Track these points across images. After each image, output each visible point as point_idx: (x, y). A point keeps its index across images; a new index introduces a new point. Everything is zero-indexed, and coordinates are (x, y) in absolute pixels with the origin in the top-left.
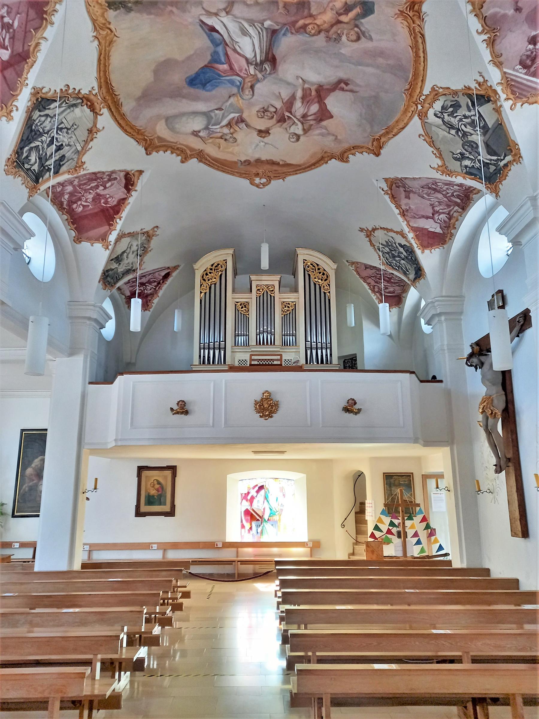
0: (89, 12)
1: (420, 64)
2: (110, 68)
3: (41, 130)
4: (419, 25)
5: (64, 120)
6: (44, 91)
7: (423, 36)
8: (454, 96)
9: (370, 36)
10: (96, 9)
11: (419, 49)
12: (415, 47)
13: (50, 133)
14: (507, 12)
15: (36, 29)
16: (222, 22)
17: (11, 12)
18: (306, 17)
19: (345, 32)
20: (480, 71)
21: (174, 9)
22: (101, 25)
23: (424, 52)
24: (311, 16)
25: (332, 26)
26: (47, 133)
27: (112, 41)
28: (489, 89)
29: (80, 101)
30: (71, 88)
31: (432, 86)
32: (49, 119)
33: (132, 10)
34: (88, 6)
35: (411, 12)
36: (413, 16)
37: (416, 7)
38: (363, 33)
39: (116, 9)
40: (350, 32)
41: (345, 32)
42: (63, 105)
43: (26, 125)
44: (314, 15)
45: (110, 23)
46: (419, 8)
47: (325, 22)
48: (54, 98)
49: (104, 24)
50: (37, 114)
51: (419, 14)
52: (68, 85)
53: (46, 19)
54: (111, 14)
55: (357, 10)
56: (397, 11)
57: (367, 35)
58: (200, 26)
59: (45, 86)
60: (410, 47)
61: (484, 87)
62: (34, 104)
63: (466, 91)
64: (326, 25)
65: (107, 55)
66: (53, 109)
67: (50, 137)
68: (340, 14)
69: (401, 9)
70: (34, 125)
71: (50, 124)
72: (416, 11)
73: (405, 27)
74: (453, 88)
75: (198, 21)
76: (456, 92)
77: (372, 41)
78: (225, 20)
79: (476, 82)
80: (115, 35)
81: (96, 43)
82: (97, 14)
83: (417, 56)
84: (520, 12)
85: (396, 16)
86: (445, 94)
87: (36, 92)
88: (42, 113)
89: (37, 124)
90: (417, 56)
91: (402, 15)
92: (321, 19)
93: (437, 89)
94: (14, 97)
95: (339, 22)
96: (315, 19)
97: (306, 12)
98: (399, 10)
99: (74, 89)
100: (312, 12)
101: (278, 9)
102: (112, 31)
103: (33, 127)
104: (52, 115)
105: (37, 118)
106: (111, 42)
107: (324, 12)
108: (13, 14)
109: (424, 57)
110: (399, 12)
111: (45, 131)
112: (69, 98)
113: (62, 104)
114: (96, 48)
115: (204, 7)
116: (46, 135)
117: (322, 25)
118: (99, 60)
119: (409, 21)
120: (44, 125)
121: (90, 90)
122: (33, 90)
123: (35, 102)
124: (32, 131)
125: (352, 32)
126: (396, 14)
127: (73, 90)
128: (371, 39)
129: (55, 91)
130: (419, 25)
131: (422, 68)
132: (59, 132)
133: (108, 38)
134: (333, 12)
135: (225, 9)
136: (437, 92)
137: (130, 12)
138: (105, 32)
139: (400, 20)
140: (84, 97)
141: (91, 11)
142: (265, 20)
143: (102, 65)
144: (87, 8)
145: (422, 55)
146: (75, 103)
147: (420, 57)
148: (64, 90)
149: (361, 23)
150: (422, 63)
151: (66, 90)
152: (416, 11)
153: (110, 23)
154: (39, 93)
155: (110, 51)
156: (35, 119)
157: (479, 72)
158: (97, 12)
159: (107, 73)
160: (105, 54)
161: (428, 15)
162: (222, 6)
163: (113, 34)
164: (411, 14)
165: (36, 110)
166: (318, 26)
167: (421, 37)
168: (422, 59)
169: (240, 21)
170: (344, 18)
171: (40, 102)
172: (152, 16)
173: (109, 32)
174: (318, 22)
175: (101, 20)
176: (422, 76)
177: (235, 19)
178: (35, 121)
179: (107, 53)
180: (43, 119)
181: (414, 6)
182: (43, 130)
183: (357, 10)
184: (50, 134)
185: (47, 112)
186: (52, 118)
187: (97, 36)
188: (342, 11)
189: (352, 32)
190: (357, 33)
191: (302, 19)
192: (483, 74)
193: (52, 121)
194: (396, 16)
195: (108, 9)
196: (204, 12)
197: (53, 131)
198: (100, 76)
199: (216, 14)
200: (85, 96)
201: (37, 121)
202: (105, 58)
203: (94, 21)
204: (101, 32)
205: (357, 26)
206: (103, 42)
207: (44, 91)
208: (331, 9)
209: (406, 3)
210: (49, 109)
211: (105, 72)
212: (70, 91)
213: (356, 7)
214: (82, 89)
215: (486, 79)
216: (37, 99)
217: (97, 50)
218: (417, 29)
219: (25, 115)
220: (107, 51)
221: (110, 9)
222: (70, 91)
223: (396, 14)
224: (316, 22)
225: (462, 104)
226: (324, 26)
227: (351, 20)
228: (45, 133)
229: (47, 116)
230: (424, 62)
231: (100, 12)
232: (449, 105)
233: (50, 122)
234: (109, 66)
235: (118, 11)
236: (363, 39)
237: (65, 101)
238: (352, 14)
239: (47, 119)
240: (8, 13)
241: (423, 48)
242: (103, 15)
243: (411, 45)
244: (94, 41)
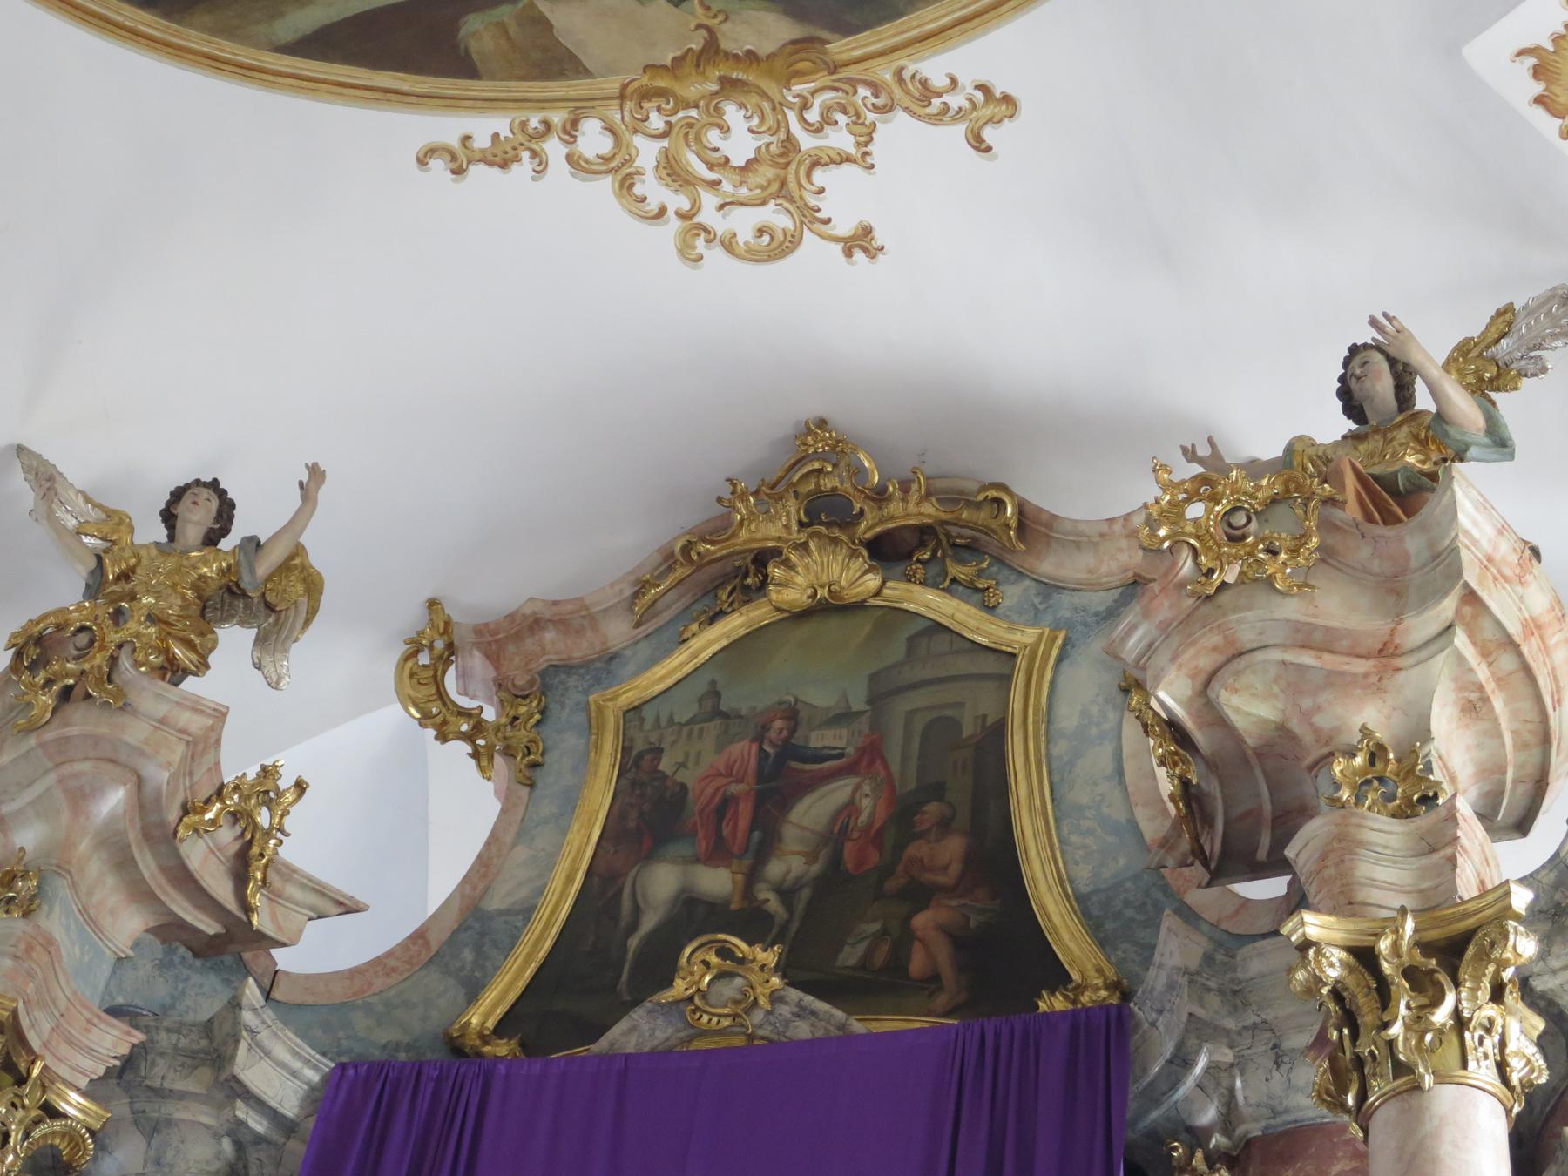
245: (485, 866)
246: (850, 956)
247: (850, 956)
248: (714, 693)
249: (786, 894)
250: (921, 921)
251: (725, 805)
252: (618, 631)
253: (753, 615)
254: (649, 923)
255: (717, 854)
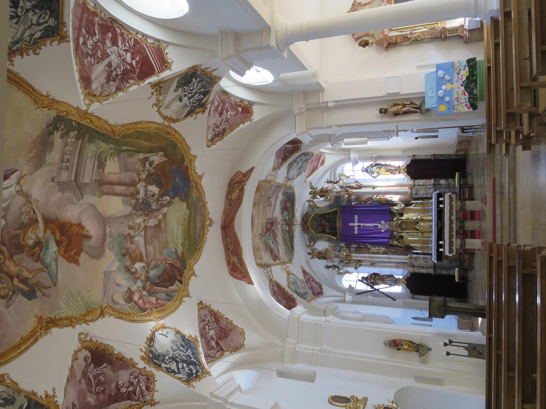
0: (65, 103)
1: (14, 352)
2: (15, 87)
3: (37, 11)
4: (41, 333)
5: (16, 26)
6: (56, 42)
7: (36, 340)
8: (16, 392)
9: (10, 305)
10: (63, 108)
11: (25, 344)
12: (24, 341)
13: (24, 11)
14: (78, 377)
15: (80, 69)
16: (11, 186)
17: (90, 64)
18: (10, 252)
19: (5, 285)
20: (55, 388)
21: (32, 154)
22: (52, 104)
23: (27, 349)
24: (11, 256)
25: (7, 274)
26: (27, 11)
27: (36, 103)
28: (53, 403)
29: (15, 48)
30: (32, 54)
31: (3, 373)
32: (34, 22)
33: (46, 128)
34: (68, 105)
35: (45, 323)
36: (44, 326)
37: (50, 325)
38: (10, 299)
39: (54, 118)
40: (6, 289)
41: (5, 285)
42: (28, 39)
43: (58, 13)
44: (12, 258)
45: (49, 110)
46: (51, 327)
47: (8, 267)
48: (43, 41)
49: (51, 106)
50: (52, 22)
51: (47, 329)
52: (37, 55)
53: (80, 80)
54: (53, 114)
55: (26, 289)
56: (40, 314)
57: (10, 303)
58: (12, 169)
59: (59, 46)
60: (22, 337)
61: (49, 400)
62: (59, 30)
63: (30, 395)
64: (6, 269)
65: (29, 94)
66: (36, 32)
67: (22, 7)
68: (18, 277)
69: (43, 317)
70: (48, 14)
71: (30, 19)
72: (48, 326)
73: (33, 325)
74: (21, 386)
75: (17, 169)
76: (20, 391)
77: (6, 309)
78: (12, 189)
79: (45, 393)
80: (39, 108)
81: (44, 93)
82: (60, 107)
83: (19, 346)
84: (80, 384)
85: (36, 316)
86: (8, 387)
87: (64, 38)
88: (45, 25)
89: (46, 15)
90: (19, 346)
91: (40, 320)
92: (11, 264)
93: (7, 378)
94: (73, 24)
95: (12, 278)
96: (9, 259)
97: (13, 251)
98: (41, 316)
99: (29, 55)
100: (15, 256)
101: (15, 230)
102: (43, 107)
103: (48, 12)
104: (33, 27)
105: (48, 20)
106: (36, 102)
107: (16, 264)
108: (89, 63)
109: (22, 351)
110: (40, 316)
111: (31, 11)
112: (27, 46)
113: (30, 39)
114: (41, 91)
115: (27, 176)
116: (28, 8)
117: (5, 266)
118: (30, 86)
119: (39, 325)
120: (37, 16)
121: (13, 62)
122: (68, 39)
123: (59, 32)
124: (49, 8)
125: (6, 291)
126: (37, 315)
127: (29, 53)
128: (8, 307)
129: (45, 46)
130: (41, 333)
131: (12, 355)
132: (14, 14)
133: (41, 102)
134: (18, 271)
135: (21, 190)
136: (3, 380)
137: (46, 126)
138: (45, 103)
139: (36, 320)
140: (14, 54)
141: (64, 105)
142: (6, 220)
143: (25, 85)
144: (68, 104)
145: (23, 348)
146: (17, 45)
147: (20, 348)
148: (38, 50)
149: (18, 295)
150: (16, 353)
151: (35, 51)
152: (48, 326)
153: (49, 110)
154: (60, 39)
155: (30, 97)
156: (51, 19)
157: (53, 388)
158: (61, 108)
159: (14, 83)
160: (30, 93)
161: (51, 334)
162: (24, 189)
163: (41, 107)
164: (44, 324)
165: (54, 26)
166: (4, 263)
167: (34, 339)
168: (20, 350)
169: (9, 200)
170: (16, 281)
171: (54, 33)
172: (35, 137)
173: (44, 106)
174: (7, 263)
175: (55, 106)
176: (6, 360)
177: (11, 196)
178: (50, 17)
179: (30, 94)
180: (41, 21)
181: (49, 323)
182: (34, 11)
183: (26, 289)
184: (23, 10)
185: (41, 27)
186: (32, 24)
187: (48, 97)
188: (21, 278)
189: (6, 291)
190: (8, 295)
191: (8, 249)
192: (56, 391)
193: (30, 22)
194: (36, 316)
195: (58, 114)
196: (22, 175)
197: (21, 13)
198: (16, 77)
199: (18, 183)
200: (13, 56)
201: (47, 18)
202: (28, 90)
203: (58, 102)
204: (48, 101)
205: (14, 292)
206: (41, 98)
207: (56, 42)
208: (20, 270)
209: (48, 317)
210: (41, 31)
211: (17, 83)
212: (31, 51)
213: (28, 287)
214: (21, 58)
215: (56, 395)
216: (58, 34)
217: (40, 91)
218: (38, 334)
219: (65, 20)
220: (32, 95)
221: (57, 115)
222: (31, 51)
223: (37, 315)
224: (7, 260)
225: (16, 402)
226: (5, 267)
227: (17, 286)
228: (30, 9)
229: (39, 24)
230: (18, 354)
231: (60, 109)
232: (3, 397)
233: (31, 21)
234: (19, 88)
235: (52, 119)
236: (4, 301)
237: (29, 42)
238: (21, 286)
239: (37, 22)
240: (91, 62)
241: (28, 346)
242: (57, 109)
243: (23, 338)
244: (47, 93)
245: (325, 240)
246: (333, 220)
247: (333, 220)
248: (315, 229)
249: (329, 224)
250: (331, 217)
251: (323, 228)
252: (309, 235)
253: (310, 227)
254: (330, 231)
255: (326, 228)
